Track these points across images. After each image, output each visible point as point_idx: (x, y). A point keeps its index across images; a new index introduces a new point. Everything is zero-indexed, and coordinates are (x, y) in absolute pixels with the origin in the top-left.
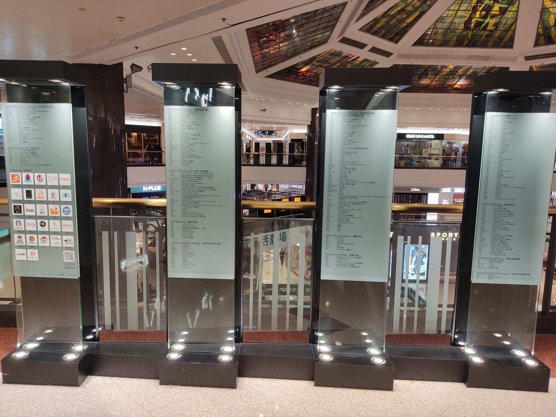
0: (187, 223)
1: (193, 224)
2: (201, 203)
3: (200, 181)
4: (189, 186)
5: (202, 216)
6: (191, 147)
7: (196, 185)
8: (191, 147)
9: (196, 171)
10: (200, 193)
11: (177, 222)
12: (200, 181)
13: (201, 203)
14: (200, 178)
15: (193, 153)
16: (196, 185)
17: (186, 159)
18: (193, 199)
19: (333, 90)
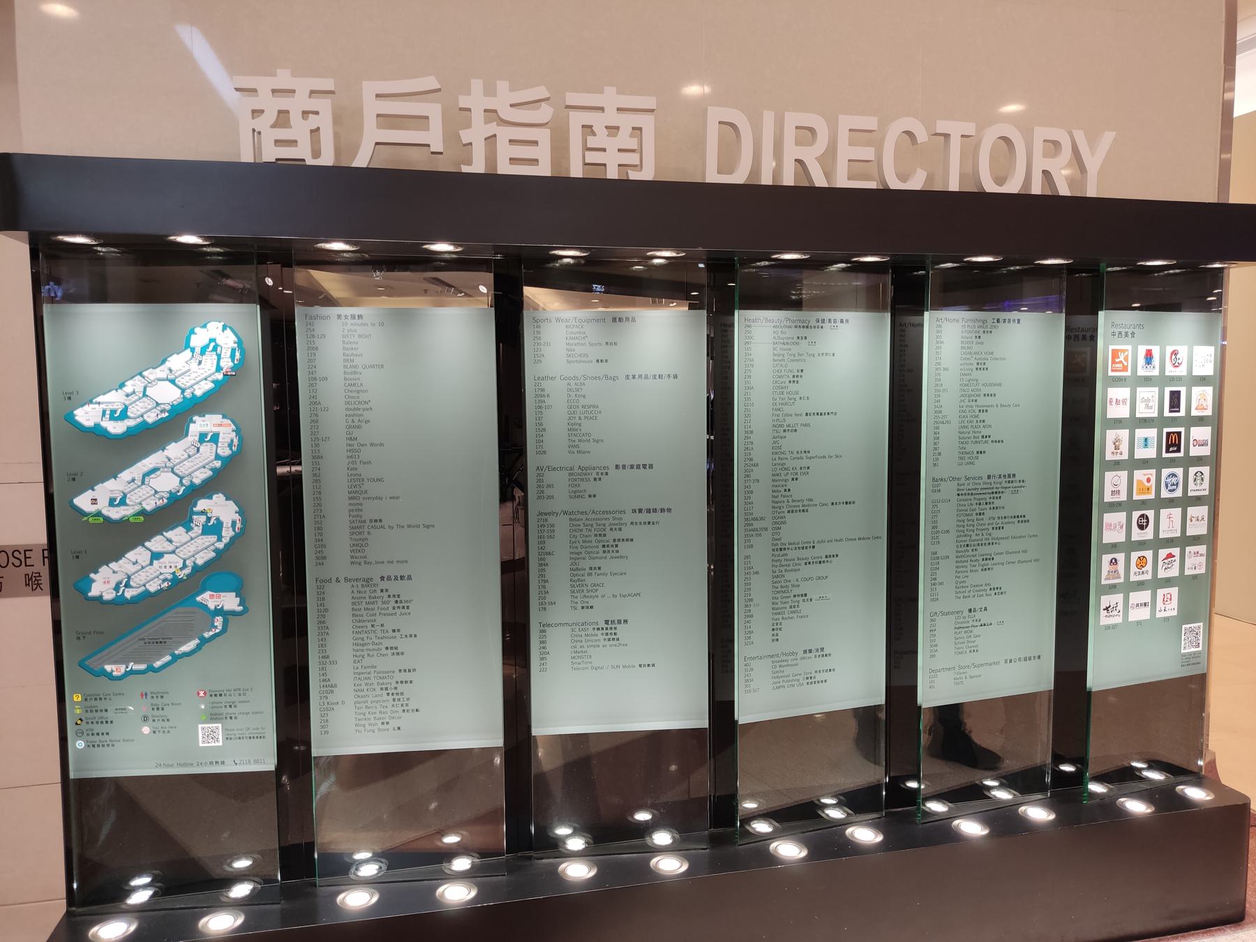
0: (966, 613)
1: (978, 615)
2: (997, 559)
3: (997, 503)
4: (975, 517)
5: (998, 591)
6: (982, 416)
7: (989, 513)
8: (982, 416)
9: (989, 477)
10: (996, 534)
11: (943, 614)
12: (997, 503)
13: (997, 559)
14: (997, 494)
15: (985, 432)
16: (989, 513)
17: (969, 448)
18: (983, 550)
19: (656, 261)
